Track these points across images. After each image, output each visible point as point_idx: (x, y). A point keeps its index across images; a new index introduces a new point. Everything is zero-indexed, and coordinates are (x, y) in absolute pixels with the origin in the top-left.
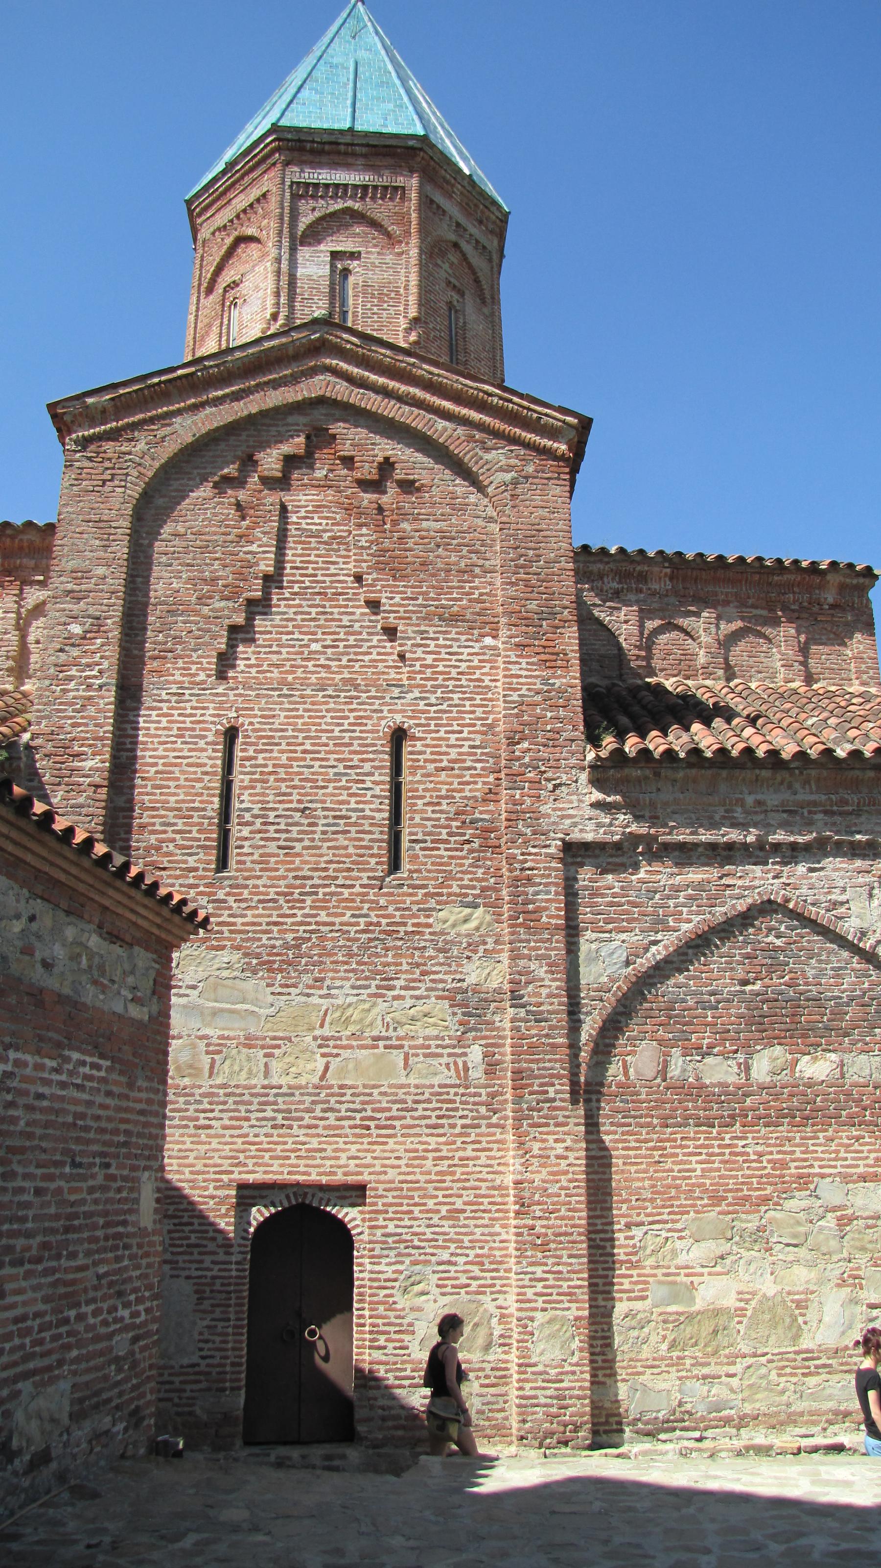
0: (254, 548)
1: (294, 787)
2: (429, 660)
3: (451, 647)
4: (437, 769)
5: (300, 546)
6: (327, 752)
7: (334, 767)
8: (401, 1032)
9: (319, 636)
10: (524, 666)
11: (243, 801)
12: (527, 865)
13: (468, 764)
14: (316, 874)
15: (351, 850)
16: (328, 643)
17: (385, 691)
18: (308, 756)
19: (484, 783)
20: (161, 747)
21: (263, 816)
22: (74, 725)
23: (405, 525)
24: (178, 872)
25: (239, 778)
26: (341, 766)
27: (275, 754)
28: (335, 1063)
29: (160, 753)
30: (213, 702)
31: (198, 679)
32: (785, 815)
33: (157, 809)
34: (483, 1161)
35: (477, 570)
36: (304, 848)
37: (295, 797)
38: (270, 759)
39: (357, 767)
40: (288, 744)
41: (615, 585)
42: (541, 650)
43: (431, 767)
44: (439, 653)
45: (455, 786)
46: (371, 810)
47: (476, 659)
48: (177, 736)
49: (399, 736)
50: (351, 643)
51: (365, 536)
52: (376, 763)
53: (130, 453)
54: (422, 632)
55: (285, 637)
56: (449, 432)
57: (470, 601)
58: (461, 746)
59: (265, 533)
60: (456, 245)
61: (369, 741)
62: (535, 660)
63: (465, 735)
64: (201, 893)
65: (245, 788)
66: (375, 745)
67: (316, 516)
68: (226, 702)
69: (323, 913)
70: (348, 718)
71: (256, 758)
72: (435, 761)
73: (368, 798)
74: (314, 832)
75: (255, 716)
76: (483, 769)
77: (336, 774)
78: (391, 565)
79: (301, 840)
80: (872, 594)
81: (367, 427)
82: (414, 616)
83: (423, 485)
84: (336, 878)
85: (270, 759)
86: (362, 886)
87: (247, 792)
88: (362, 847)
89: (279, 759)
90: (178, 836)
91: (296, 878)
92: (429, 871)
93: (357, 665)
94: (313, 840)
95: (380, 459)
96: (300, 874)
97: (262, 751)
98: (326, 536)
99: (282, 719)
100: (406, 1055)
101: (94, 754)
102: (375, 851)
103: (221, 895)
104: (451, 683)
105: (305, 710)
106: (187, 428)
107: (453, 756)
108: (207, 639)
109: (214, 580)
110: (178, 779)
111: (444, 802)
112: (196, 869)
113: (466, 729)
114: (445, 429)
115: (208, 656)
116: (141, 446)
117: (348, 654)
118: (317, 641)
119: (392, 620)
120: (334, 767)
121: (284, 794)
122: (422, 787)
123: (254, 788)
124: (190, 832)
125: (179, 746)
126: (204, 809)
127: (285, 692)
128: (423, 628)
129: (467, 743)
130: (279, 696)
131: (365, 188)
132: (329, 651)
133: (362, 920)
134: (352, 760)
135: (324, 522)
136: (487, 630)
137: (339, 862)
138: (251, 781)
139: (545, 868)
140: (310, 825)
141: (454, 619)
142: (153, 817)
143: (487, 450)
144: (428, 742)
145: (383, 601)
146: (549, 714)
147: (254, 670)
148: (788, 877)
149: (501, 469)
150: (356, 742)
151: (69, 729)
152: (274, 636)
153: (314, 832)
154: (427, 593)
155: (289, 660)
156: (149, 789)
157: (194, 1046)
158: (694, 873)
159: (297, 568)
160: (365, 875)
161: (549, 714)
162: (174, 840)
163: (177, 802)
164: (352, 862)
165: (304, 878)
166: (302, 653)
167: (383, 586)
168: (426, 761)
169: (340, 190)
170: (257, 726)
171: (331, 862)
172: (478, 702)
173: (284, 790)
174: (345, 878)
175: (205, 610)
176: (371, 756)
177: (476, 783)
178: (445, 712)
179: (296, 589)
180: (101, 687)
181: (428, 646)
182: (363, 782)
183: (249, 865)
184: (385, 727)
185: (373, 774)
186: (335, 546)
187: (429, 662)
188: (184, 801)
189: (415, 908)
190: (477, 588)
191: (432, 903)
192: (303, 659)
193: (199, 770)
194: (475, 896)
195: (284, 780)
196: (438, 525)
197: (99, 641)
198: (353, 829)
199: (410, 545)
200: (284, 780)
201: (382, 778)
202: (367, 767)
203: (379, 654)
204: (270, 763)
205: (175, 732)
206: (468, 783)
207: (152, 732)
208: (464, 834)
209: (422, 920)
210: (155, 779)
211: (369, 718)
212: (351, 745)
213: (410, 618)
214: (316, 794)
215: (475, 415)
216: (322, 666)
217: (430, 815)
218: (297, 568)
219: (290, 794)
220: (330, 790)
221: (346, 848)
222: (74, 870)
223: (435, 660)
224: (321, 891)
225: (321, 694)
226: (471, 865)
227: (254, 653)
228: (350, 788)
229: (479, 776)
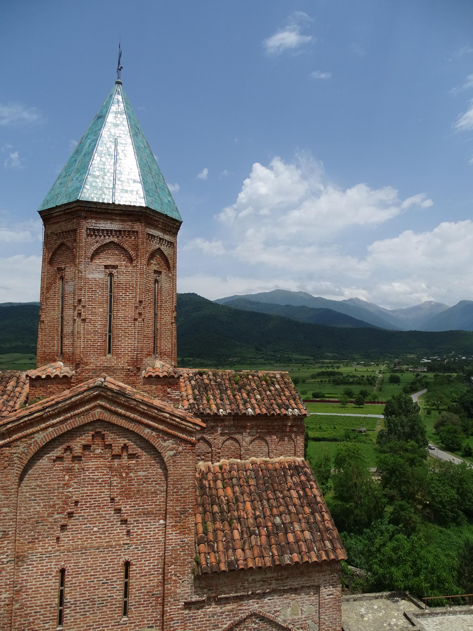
0: (71, 490)
1: (87, 590)
3: (147, 525)
4: (140, 576)
5: (90, 486)
6: (100, 575)
7: (102, 580)
9: (97, 524)
10: (174, 535)
11: (68, 598)
12: (171, 613)
13: (152, 573)
14: (95, 623)
15: (108, 612)
17: (122, 547)
18: (92, 577)
19: (158, 579)
20: (34, 581)
26: (105, 579)
27: (80, 578)
29: (34, 583)
30: (55, 559)
31: (48, 550)
32: (262, 582)
33: (33, 607)
35: (158, 492)
36: (90, 614)
37: (87, 594)
38: (78, 580)
40: (85, 573)
41: (212, 424)
44: (143, 529)
46: (116, 596)
47: (156, 529)
48: (40, 575)
49: (127, 564)
51: (116, 481)
52: (119, 577)
53: (16, 453)
54: (137, 521)
55: (83, 526)
58: (150, 566)
60: (159, 249)
61: (116, 568)
62: (178, 531)
63: (151, 561)
65: (68, 593)
66: (118, 569)
67: (96, 472)
68: (60, 558)
70: (107, 560)
71: (72, 581)
72: (140, 573)
73: (115, 591)
75: (72, 563)
76: (157, 574)
77: (103, 583)
78: (127, 494)
82: (134, 514)
83: (139, 456)
85: (78, 580)
86: (112, 626)
87: (68, 595)
88: (112, 611)
89: (81, 580)
90: (41, 617)
91: (87, 626)
92: (136, 616)
93: (112, 535)
95: (122, 445)
98: (100, 480)
99: (82, 563)
101: (6, 591)
102: (117, 612)
104: (147, 541)
105: (91, 558)
106: (41, 438)
107: (147, 570)
108: (51, 532)
110: (41, 593)
111: (143, 589)
113: (152, 559)
114: (148, 432)
115: (52, 540)
116: (21, 449)
117: (108, 531)
119: (125, 516)
120: (102, 580)
122: (135, 584)
123: (71, 593)
124: (46, 614)
125: (41, 579)
126: (52, 604)
127: (84, 551)
128: (137, 519)
129: (152, 565)
130: (81, 553)
131: (120, 231)
132: (101, 530)
134: (109, 577)
135: (99, 474)
136: (161, 517)
137: (103, 618)
138: (70, 590)
139: (178, 614)
140: (93, 605)
142: (31, 610)
143: (165, 441)
144: (138, 565)
145: (122, 509)
146: (182, 553)
148: (261, 604)
150: (110, 569)
152: (79, 526)
154: (139, 503)
155: (85, 536)
156: (29, 599)
158: (229, 606)
159: (88, 496)
161: (182, 553)
162: (39, 618)
163: (41, 603)
164: (108, 617)
166: (90, 532)
167: (122, 502)
168: (137, 573)
169: (109, 232)
170: (72, 567)
173: (83, 592)
174: (106, 624)
175: (50, 519)
176: (116, 574)
177: (154, 580)
178: (144, 553)
179: (88, 505)
180: (8, 562)
181: (139, 526)
182: (113, 585)
185: (117, 581)
186: (103, 485)
187: (139, 533)
188: (43, 602)
190: (158, 500)
192: (91, 535)
193: (49, 588)
194: (152, 624)
195: (83, 588)
196: (144, 473)
197: (6, 542)
199: (133, 483)
200: (83, 588)
202: (115, 579)
203: (120, 530)
204: (78, 582)
205: (39, 574)
206: (152, 580)
207: (30, 575)
208: (150, 600)
210: (32, 594)
212: (109, 570)
213: (132, 515)
214: (95, 592)
215: (161, 427)
216: (98, 537)
217: (138, 595)
218: (88, 496)
219: (85, 594)
221: (106, 612)
223: (141, 532)
225: (97, 551)
227: (71, 534)
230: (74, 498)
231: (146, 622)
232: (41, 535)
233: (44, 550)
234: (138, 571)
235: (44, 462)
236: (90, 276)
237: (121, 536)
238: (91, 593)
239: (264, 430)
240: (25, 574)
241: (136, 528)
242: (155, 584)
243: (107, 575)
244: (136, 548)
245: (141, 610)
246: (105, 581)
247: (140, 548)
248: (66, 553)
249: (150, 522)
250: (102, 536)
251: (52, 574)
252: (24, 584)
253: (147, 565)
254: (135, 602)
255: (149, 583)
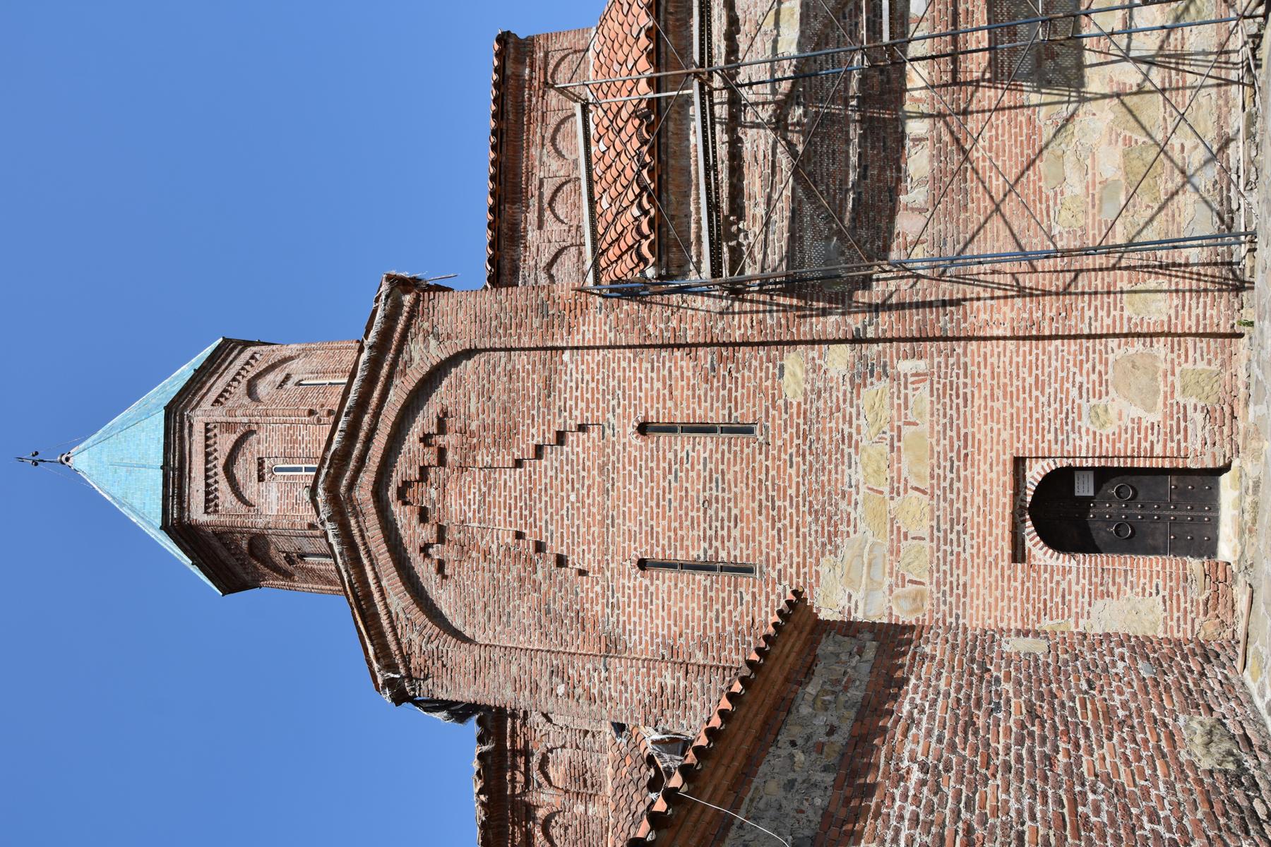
0: (494, 547)
1: (687, 514)
2: (582, 405)
8: (886, 428)
9: (564, 494)
13: (666, 373)
14: (757, 497)
15: (737, 468)
16: (569, 486)
18: (661, 503)
21: (711, 540)
22: (638, 691)
23: (474, 426)
24: (756, 609)
25: (681, 556)
27: (660, 530)
28: (913, 482)
29: (659, 622)
31: (600, 591)
33: (705, 625)
34: (995, 360)
35: (509, 367)
37: (695, 514)
39: (670, 464)
42: (572, 314)
43: (669, 404)
45: (684, 383)
47: (580, 367)
49: (643, 429)
50: (569, 468)
51: (483, 457)
52: (667, 447)
54: (560, 411)
55: (565, 522)
56: (398, 390)
57: (534, 372)
59: (482, 538)
61: (649, 454)
63: (643, 376)
64: (773, 590)
65: (687, 553)
69: (789, 492)
72: (664, 400)
74: (723, 499)
78: (508, 434)
79: (730, 509)
80: (522, 36)
81: (396, 457)
84: (760, 480)
87: (691, 553)
90: (727, 608)
92: (754, 406)
93: (587, 463)
94: (729, 500)
96: (757, 510)
97: (658, 541)
98: (484, 489)
99: (632, 524)
100: (907, 423)
102: (738, 449)
103: (775, 575)
104: (601, 387)
107: (660, 385)
108: (568, 585)
109: (521, 579)
110: (681, 608)
111: (697, 392)
112: (754, 594)
116: (414, 636)
118: (568, 496)
119: (551, 436)
121: (692, 523)
125: (654, 607)
127: (609, 521)
129: (650, 374)
132: (576, 486)
133: (794, 459)
138: (682, 549)
140: (717, 502)
141: (549, 386)
144: (649, 405)
147: (593, 547)
149: (427, 347)
150: (650, 465)
151: (640, 695)
153: (723, 499)
156: (689, 631)
157: (897, 597)
160: (758, 458)
162: (730, 612)
164: (748, 467)
165: (760, 505)
168: (664, 408)
171: (747, 485)
172: (616, 365)
173: (689, 523)
174: (760, 473)
175: (544, 587)
179: (527, 513)
183: (750, 552)
184: (638, 441)
187: (584, 405)
188: (699, 604)
189: (784, 416)
191: (781, 402)
194: (774, 368)
195: (681, 523)
196: (474, 399)
198: (720, 467)
200: (681, 523)
201: (679, 443)
202: (670, 455)
205: (643, 611)
206: (682, 373)
209: (795, 410)
210: (681, 627)
211: (630, 453)
217: (708, 404)
219: (692, 518)
220: (689, 485)
221: (736, 472)
222: (755, 708)
224: (770, 493)
226: (749, 370)
228: (687, 470)
229: (676, 363)
230: (510, 540)
231: (769, 383)
232: (572, 606)
233: (600, 600)
234: (660, 406)
235: (444, 598)
236: (275, 508)
237: (590, 444)
238: (692, 505)
239: (538, 130)
240: (641, 638)
241: (574, 413)
242: (691, 364)
243: (661, 472)
244: (614, 411)
245: (743, 394)
246: (671, 477)
247: (615, 402)
248: (609, 557)
249: (566, 382)
250: (586, 483)
251: (647, 587)
252: (660, 640)
253: (648, 386)
254: (724, 408)
255: (688, 378)
